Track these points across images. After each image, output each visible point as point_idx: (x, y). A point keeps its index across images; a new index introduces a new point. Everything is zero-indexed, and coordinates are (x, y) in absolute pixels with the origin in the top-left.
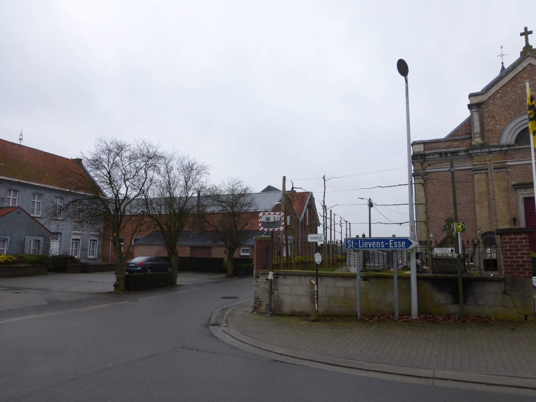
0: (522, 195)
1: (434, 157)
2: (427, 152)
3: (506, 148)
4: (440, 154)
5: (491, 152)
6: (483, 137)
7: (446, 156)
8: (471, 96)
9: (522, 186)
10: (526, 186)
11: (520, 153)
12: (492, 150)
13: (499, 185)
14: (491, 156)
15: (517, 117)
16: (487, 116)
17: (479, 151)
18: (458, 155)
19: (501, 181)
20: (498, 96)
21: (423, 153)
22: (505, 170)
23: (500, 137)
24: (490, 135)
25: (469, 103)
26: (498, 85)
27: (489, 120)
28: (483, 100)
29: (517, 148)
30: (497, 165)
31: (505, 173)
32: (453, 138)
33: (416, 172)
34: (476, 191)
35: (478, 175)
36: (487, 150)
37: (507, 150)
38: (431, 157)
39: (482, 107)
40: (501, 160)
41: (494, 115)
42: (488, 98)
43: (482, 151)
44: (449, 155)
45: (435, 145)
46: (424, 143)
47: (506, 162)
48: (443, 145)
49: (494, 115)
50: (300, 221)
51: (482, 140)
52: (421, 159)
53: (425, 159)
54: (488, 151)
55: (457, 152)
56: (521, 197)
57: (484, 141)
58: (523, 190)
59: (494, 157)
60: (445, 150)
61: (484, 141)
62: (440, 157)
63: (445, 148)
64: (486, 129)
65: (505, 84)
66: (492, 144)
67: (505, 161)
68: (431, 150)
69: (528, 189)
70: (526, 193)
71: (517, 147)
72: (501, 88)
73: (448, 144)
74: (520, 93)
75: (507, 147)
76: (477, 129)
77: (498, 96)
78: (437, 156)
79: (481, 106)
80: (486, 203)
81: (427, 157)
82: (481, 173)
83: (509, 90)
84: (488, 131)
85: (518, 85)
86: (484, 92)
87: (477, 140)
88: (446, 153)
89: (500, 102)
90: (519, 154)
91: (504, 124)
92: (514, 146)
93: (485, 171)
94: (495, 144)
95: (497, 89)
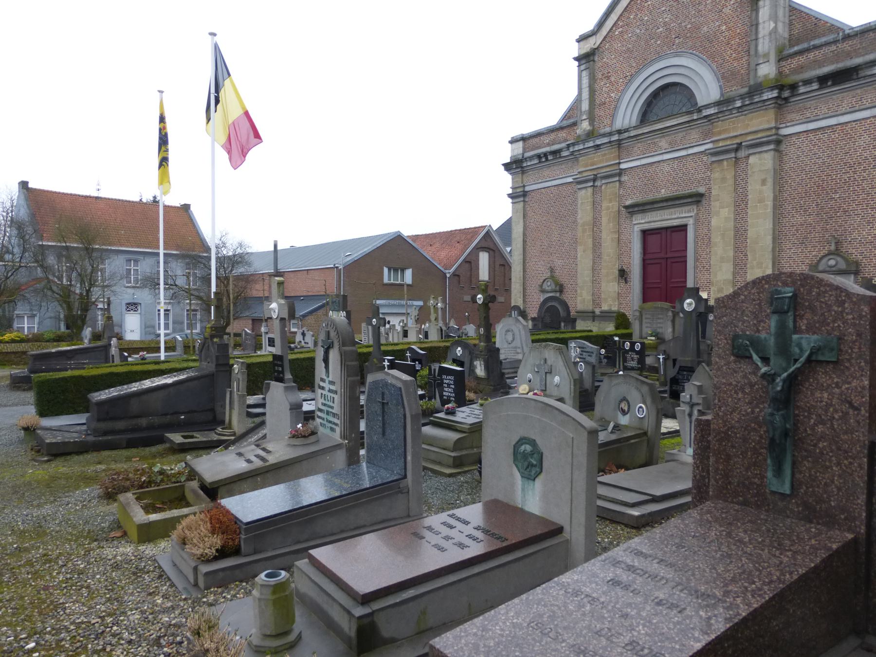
0: (639, 226)
1: (532, 163)
2: (528, 154)
3: (615, 138)
4: (539, 156)
5: (598, 147)
6: (592, 119)
7: (547, 160)
8: (582, 39)
9: (636, 209)
10: (641, 208)
11: (641, 142)
12: (598, 142)
13: (608, 208)
14: (600, 153)
15: (639, 72)
16: (600, 77)
17: (581, 147)
18: (561, 157)
19: (610, 201)
20: (617, 33)
21: (520, 157)
22: (617, 179)
23: (613, 117)
24: (602, 113)
25: (576, 55)
26: (616, 10)
27: (602, 83)
28: (596, 46)
29: (632, 135)
30: (608, 169)
31: (617, 184)
32: (565, 123)
33: (515, 191)
34: (579, 221)
35: (584, 191)
36: (591, 144)
37: (619, 140)
38: (529, 164)
39: (594, 61)
40: (614, 160)
41: (609, 72)
42: (603, 40)
43: (586, 146)
44: (550, 157)
45: (536, 140)
46: (523, 139)
47: (619, 163)
48: (546, 139)
49: (609, 72)
50: (448, 275)
51: (590, 124)
52: (516, 168)
53: (522, 167)
54: (592, 145)
55: (558, 151)
56: (637, 229)
57: (593, 126)
58: (640, 216)
59: (605, 154)
60: (547, 149)
61: (593, 126)
62: (540, 162)
63: (549, 145)
64: (598, 102)
65: (627, 6)
66: (602, 131)
67: (617, 161)
68: (532, 150)
69: (648, 214)
70: (643, 221)
71: (640, 131)
72: (621, 15)
73: (553, 136)
74: (647, 21)
75: (617, 135)
76: (585, 106)
77: (617, 33)
78: (536, 161)
79: (592, 58)
80: (590, 241)
81: (525, 165)
82: (586, 187)
83: (632, 17)
84: (600, 105)
85: (646, 4)
86: (596, 30)
87: (585, 126)
88: (545, 155)
89: (619, 45)
90: (639, 145)
91: (622, 88)
92: (628, 131)
93: (591, 184)
94: (608, 130)
95: (615, 19)
